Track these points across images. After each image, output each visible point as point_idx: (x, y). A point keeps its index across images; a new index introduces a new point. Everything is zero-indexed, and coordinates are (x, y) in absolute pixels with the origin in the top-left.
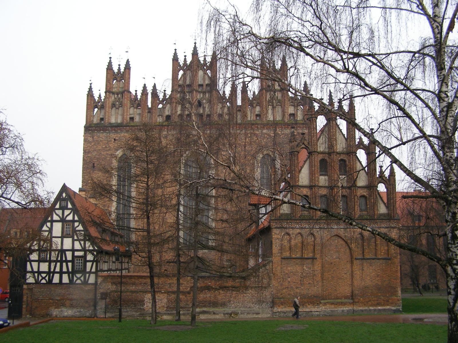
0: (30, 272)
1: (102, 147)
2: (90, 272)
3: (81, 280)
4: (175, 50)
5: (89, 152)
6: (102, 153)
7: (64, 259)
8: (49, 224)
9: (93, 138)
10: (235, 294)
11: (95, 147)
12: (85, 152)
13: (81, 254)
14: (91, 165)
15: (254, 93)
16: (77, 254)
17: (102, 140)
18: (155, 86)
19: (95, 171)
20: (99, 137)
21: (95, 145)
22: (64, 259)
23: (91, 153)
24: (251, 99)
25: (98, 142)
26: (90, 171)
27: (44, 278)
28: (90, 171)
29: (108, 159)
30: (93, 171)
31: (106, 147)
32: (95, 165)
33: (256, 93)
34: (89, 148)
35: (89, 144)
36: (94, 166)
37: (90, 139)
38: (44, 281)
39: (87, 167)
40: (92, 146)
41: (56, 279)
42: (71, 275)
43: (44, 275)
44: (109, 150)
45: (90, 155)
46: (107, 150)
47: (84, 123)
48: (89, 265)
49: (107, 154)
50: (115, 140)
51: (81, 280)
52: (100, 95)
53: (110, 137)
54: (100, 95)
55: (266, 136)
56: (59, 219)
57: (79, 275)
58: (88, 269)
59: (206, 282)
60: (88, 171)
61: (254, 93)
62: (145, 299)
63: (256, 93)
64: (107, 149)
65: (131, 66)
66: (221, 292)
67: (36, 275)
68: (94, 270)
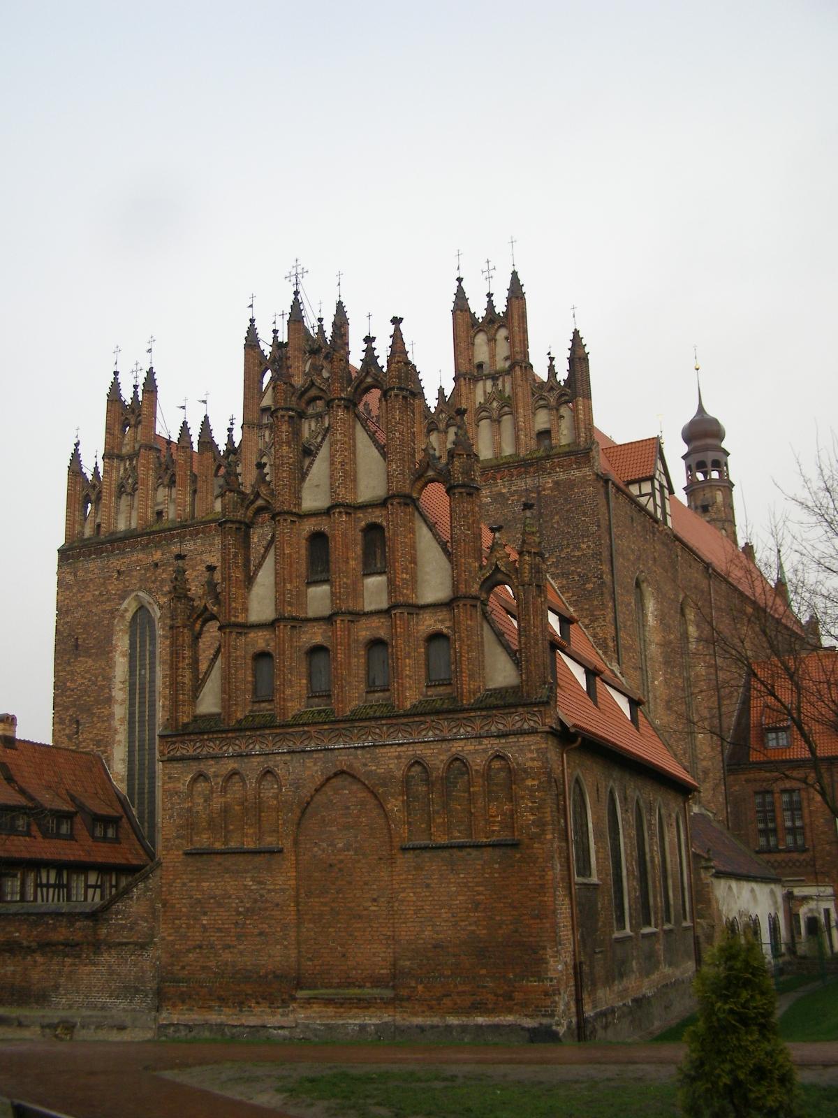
1: (93, 595)
4: (252, 320)
5: (67, 612)
9: (75, 575)
10: (71, 965)
12: (62, 611)
15: (441, 391)
17: (93, 577)
18: (206, 424)
19: (80, 656)
20: (87, 571)
21: (79, 591)
24: (433, 410)
26: (69, 659)
28: (69, 659)
29: (106, 622)
30: (77, 656)
31: (101, 594)
32: (80, 642)
33: (448, 392)
34: (67, 601)
36: (77, 646)
37: (70, 579)
39: (64, 650)
40: (74, 594)
44: (108, 600)
45: (68, 619)
47: (60, 541)
49: (104, 611)
50: (118, 572)
52: (96, 468)
53: (109, 568)
54: (96, 468)
59: (8, 929)
60: (65, 658)
61: (441, 391)
63: (448, 392)
64: (104, 598)
65: (157, 383)
66: (39, 959)
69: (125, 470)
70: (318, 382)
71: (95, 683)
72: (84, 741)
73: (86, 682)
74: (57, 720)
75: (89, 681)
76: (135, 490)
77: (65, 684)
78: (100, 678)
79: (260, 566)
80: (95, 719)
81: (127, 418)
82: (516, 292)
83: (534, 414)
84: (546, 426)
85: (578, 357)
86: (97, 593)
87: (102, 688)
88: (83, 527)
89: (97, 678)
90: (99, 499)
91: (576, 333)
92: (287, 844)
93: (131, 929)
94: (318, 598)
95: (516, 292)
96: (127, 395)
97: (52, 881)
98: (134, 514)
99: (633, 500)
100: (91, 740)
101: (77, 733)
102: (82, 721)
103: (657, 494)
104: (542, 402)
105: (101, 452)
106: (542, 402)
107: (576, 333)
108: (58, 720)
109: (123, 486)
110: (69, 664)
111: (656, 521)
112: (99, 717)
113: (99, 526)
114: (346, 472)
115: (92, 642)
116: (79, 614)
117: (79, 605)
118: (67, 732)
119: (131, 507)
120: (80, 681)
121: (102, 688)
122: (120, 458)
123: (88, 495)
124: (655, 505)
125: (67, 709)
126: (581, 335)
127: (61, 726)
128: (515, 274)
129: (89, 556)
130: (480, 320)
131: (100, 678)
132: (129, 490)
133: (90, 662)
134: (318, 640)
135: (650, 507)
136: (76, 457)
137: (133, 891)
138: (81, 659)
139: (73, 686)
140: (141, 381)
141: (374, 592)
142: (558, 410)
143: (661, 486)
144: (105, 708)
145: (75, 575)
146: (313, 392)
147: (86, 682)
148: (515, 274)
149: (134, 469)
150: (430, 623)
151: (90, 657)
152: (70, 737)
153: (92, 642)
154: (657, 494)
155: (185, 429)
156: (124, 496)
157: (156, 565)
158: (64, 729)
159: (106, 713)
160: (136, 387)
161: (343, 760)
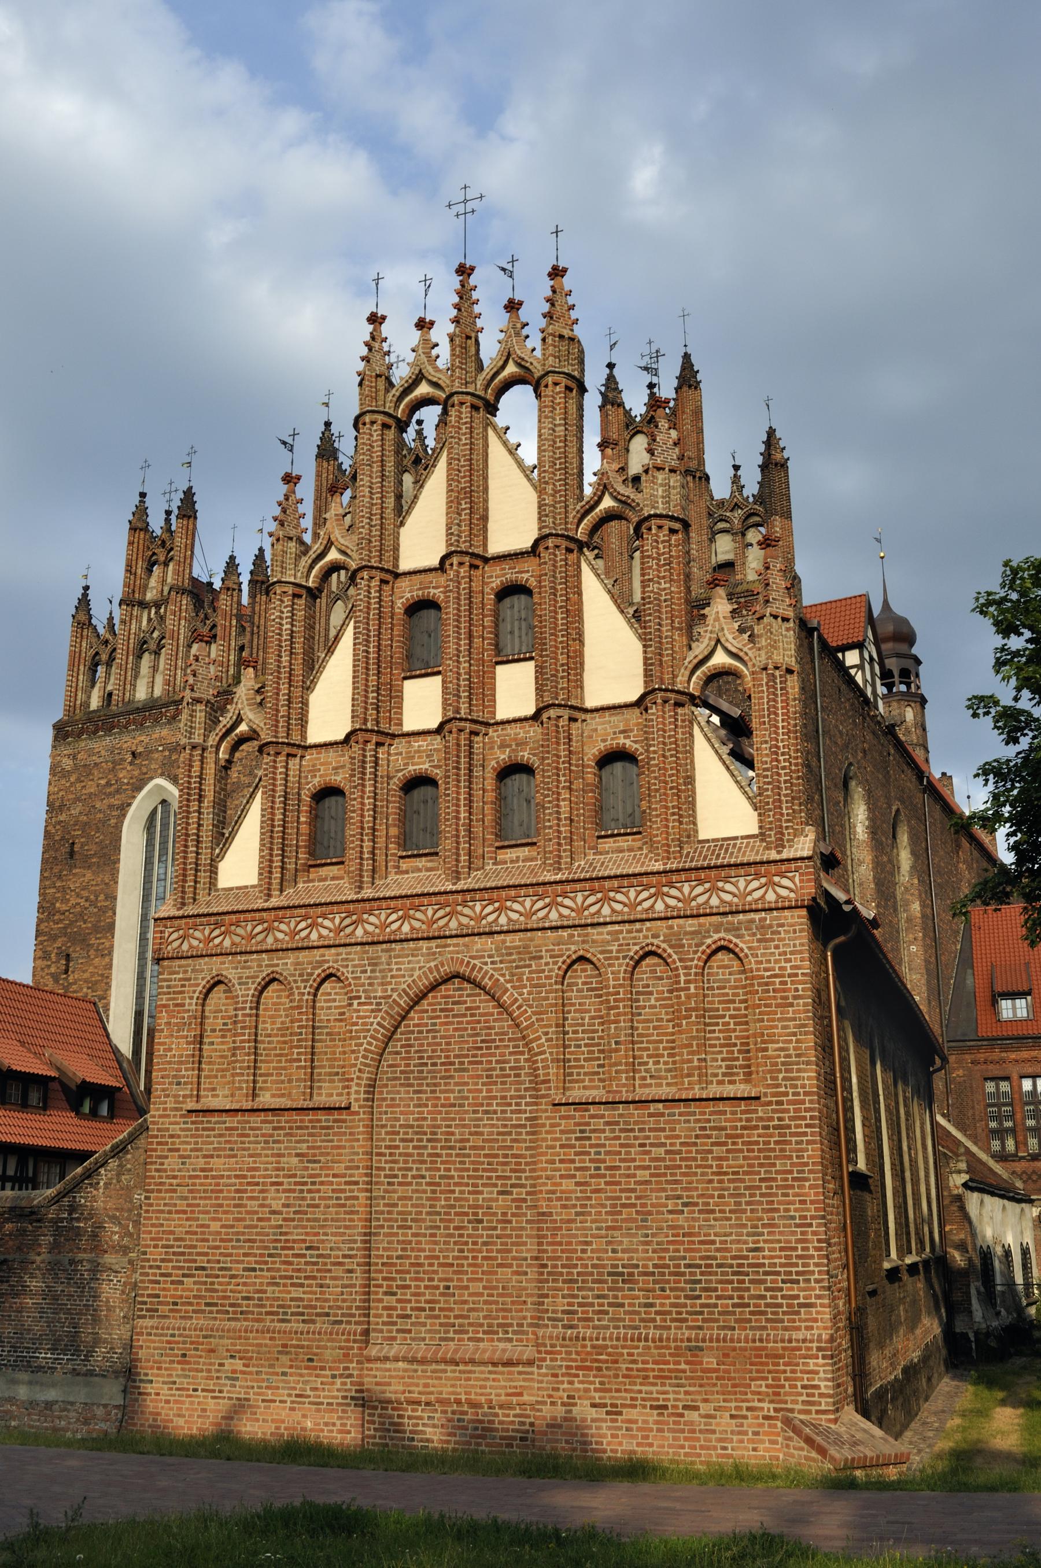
5: (61, 808)
9: (75, 758)
12: (54, 807)
14: (65, 849)
17: (98, 761)
20: (91, 753)
23: (69, 809)
25: (85, 771)
26: (61, 871)
28: (61, 871)
29: (113, 821)
30: (72, 867)
31: (109, 784)
35: (63, 782)
36: (72, 854)
37: (67, 763)
39: (55, 858)
44: (118, 791)
45: (61, 818)
46: (110, 794)
49: (111, 807)
50: (133, 754)
52: (111, 619)
53: (120, 748)
54: (111, 619)
60: (56, 870)
64: (112, 789)
69: (150, 620)
70: (428, 370)
71: (93, 904)
72: (75, 983)
73: (82, 902)
74: (40, 954)
76: (160, 647)
77: (53, 904)
78: (102, 897)
79: (330, 650)
80: (92, 952)
81: (154, 554)
82: (688, 378)
83: (712, 540)
84: (730, 557)
85: (773, 464)
86: (103, 782)
87: (103, 910)
88: (89, 697)
89: (97, 897)
90: (111, 659)
91: (771, 433)
92: (356, 1096)
94: (422, 703)
95: (688, 378)
96: (156, 523)
97: (10, 1172)
98: (159, 680)
99: (842, 669)
100: (86, 981)
101: (66, 972)
102: (73, 955)
103: (867, 667)
104: (721, 525)
105: (118, 596)
106: (721, 525)
107: (771, 433)
108: (42, 954)
109: (145, 642)
110: (60, 878)
111: (867, 701)
112: (97, 950)
113: (110, 695)
114: (470, 504)
115: (93, 848)
116: (77, 811)
117: (78, 799)
118: (53, 970)
119: (155, 669)
120: (73, 902)
121: (103, 910)
122: (143, 605)
123: (97, 654)
124: (865, 681)
125: (54, 938)
126: (778, 434)
127: (46, 963)
128: (687, 357)
129: (95, 732)
130: (638, 419)
131: (102, 897)
132: (153, 646)
133: (89, 875)
134: (423, 766)
135: (859, 679)
136: (84, 603)
137: (99, 1174)
139: (64, 907)
140: (176, 503)
141: (515, 690)
142: (744, 535)
143: (871, 658)
145: (75, 758)
146: (423, 389)
147: (82, 902)
148: (687, 357)
149: (162, 619)
150: (599, 737)
152: (56, 978)
153: (93, 848)
154: (867, 667)
155: (232, 565)
156: (146, 655)
158: (49, 967)
159: (107, 944)
160: (168, 513)
161: (453, 955)
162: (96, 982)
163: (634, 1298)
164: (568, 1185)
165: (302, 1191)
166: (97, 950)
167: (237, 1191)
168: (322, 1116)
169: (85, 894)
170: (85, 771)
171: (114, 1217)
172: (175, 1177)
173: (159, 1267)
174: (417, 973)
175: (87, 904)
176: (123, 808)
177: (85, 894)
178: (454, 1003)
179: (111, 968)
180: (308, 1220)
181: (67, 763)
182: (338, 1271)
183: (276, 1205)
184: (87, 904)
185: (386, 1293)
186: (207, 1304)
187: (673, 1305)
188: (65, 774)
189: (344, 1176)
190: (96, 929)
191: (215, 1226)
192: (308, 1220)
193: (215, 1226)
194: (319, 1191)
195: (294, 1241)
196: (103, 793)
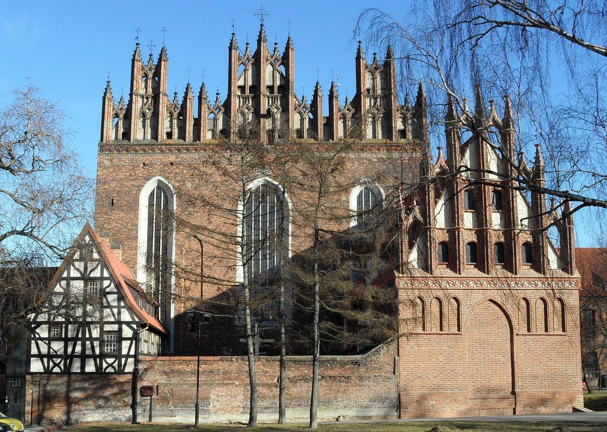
0: (34, 356)
2: (128, 356)
3: (114, 368)
5: (105, 183)
6: (125, 183)
7: (87, 336)
8: (63, 283)
10: (345, 386)
11: (114, 174)
13: (115, 327)
16: (107, 328)
21: (114, 171)
22: (87, 336)
25: (119, 168)
27: (56, 365)
31: (131, 175)
34: (104, 176)
36: (113, 203)
37: (107, 163)
38: (56, 370)
41: (76, 367)
42: (98, 360)
43: (58, 361)
44: (136, 179)
45: (106, 187)
46: (132, 180)
48: (125, 344)
49: (133, 185)
50: (144, 164)
51: (114, 368)
55: (365, 161)
56: (79, 275)
57: (110, 361)
58: (124, 352)
62: (211, 395)
64: (133, 178)
67: (45, 360)
68: (132, 352)
73: (119, 225)
75: (121, 225)
80: (126, 248)
89: (127, 224)
93: (380, 369)
110: (106, 214)
115: (124, 203)
116: (114, 185)
117: (115, 180)
120: (114, 225)
131: (130, 224)
133: (122, 214)
138: (115, 212)
144: (133, 242)
151: (122, 211)
153: (124, 203)
157: (172, 164)
159: (134, 245)
162: (129, 261)
163: (538, 382)
164: (521, 354)
165: (449, 356)
166: (129, 247)
167: (429, 356)
168: (453, 336)
169: (121, 222)
170: (119, 168)
171: (387, 363)
172: (409, 352)
173: (406, 377)
174: (480, 299)
175: (122, 227)
176: (139, 188)
177: (121, 222)
178: (488, 307)
179: (136, 255)
180: (451, 364)
181: (107, 163)
182: (461, 377)
183: (441, 360)
184: (122, 227)
185: (472, 382)
186: (422, 387)
187: (547, 383)
188: (105, 168)
189: (461, 352)
190: (127, 238)
191: (423, 365)
192: (451, 364)
193: (423, 365)
194: (454, 356)
195: (448, 369)
196: (127, 178)
